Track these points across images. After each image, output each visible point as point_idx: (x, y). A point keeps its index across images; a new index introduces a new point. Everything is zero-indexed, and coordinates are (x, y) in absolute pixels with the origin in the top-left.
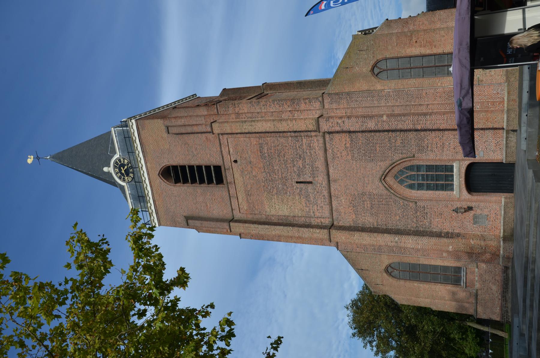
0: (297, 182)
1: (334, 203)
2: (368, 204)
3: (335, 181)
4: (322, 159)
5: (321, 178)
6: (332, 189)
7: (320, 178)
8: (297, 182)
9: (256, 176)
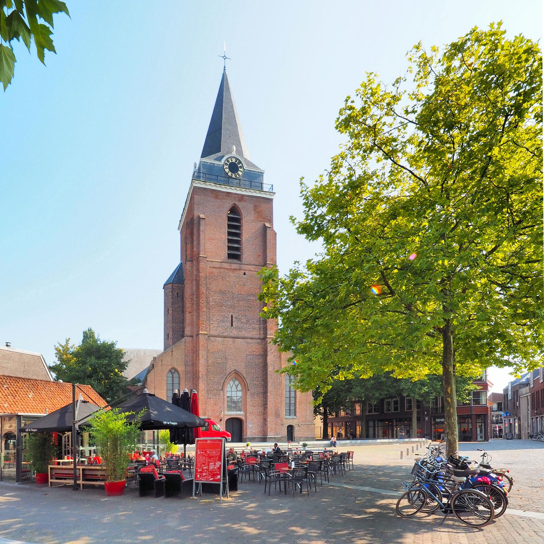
0: (232, 316)
1: (220, 339)
2: (220, 361)
3: (234, 342)
4: (246, 336)
5: (235, 333)
6: (228, 339)
7: (235, 332)
8: (232, 316)
9: (235, 286)
